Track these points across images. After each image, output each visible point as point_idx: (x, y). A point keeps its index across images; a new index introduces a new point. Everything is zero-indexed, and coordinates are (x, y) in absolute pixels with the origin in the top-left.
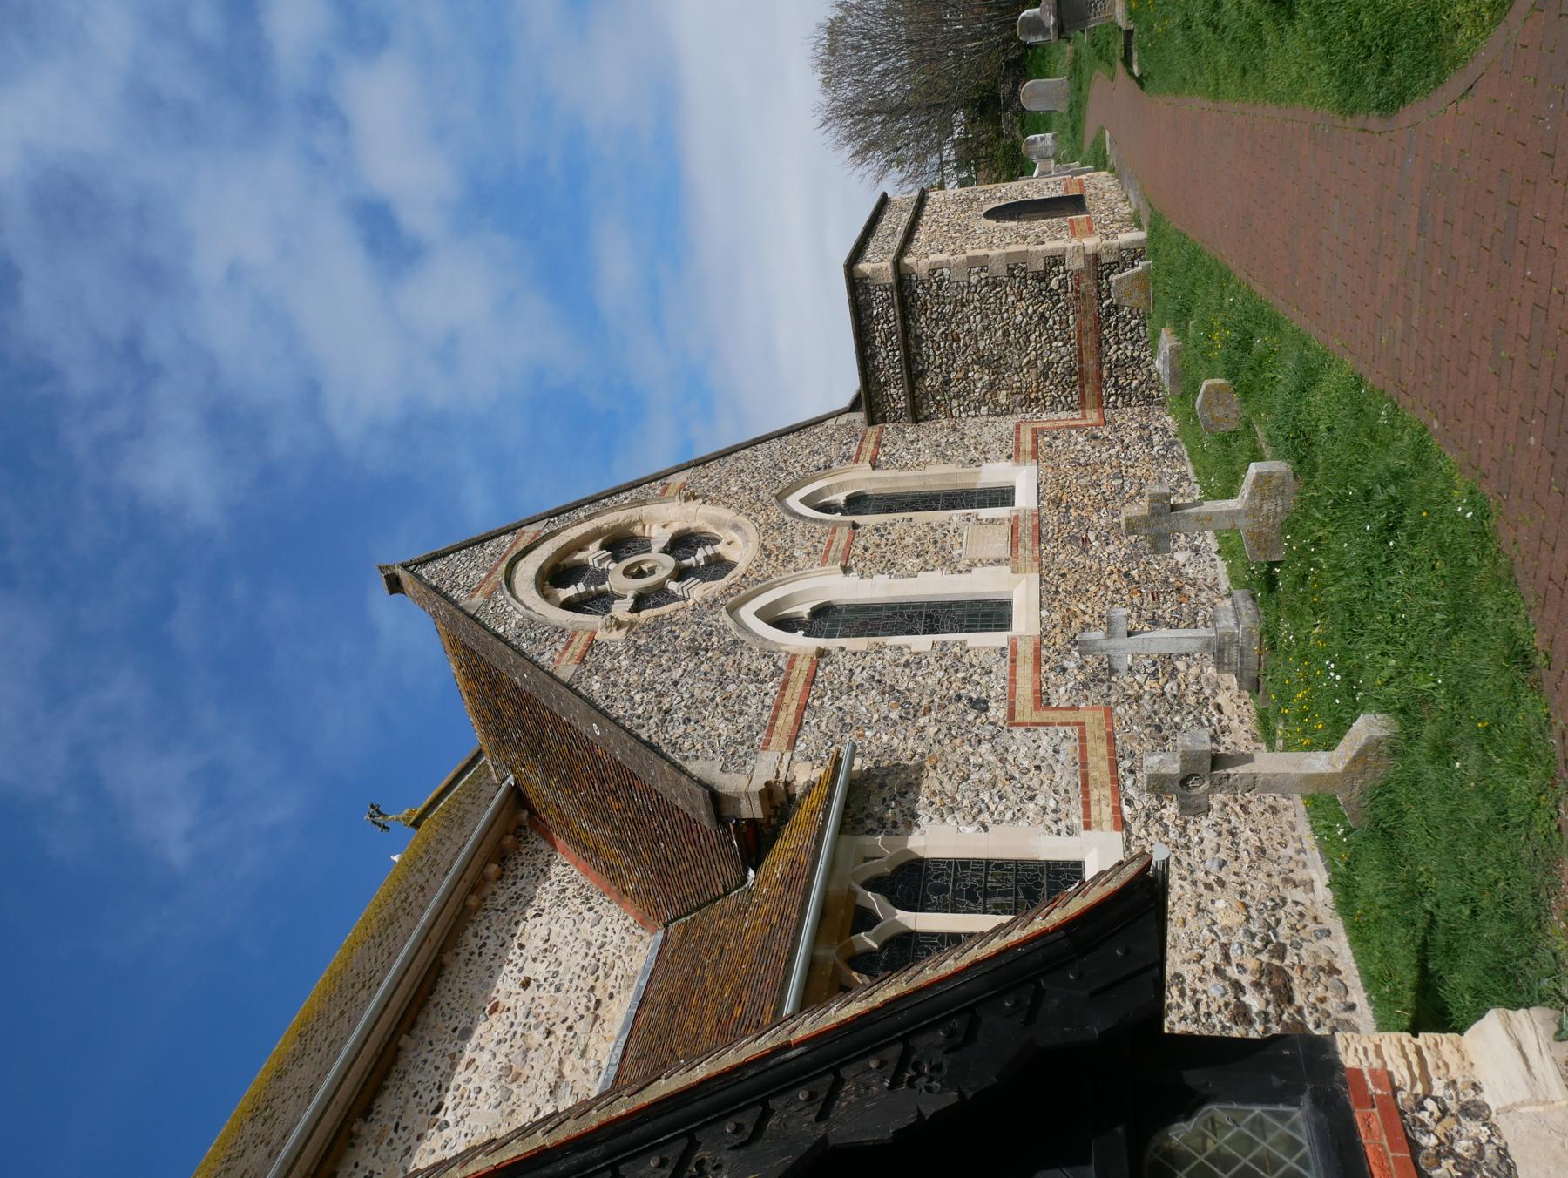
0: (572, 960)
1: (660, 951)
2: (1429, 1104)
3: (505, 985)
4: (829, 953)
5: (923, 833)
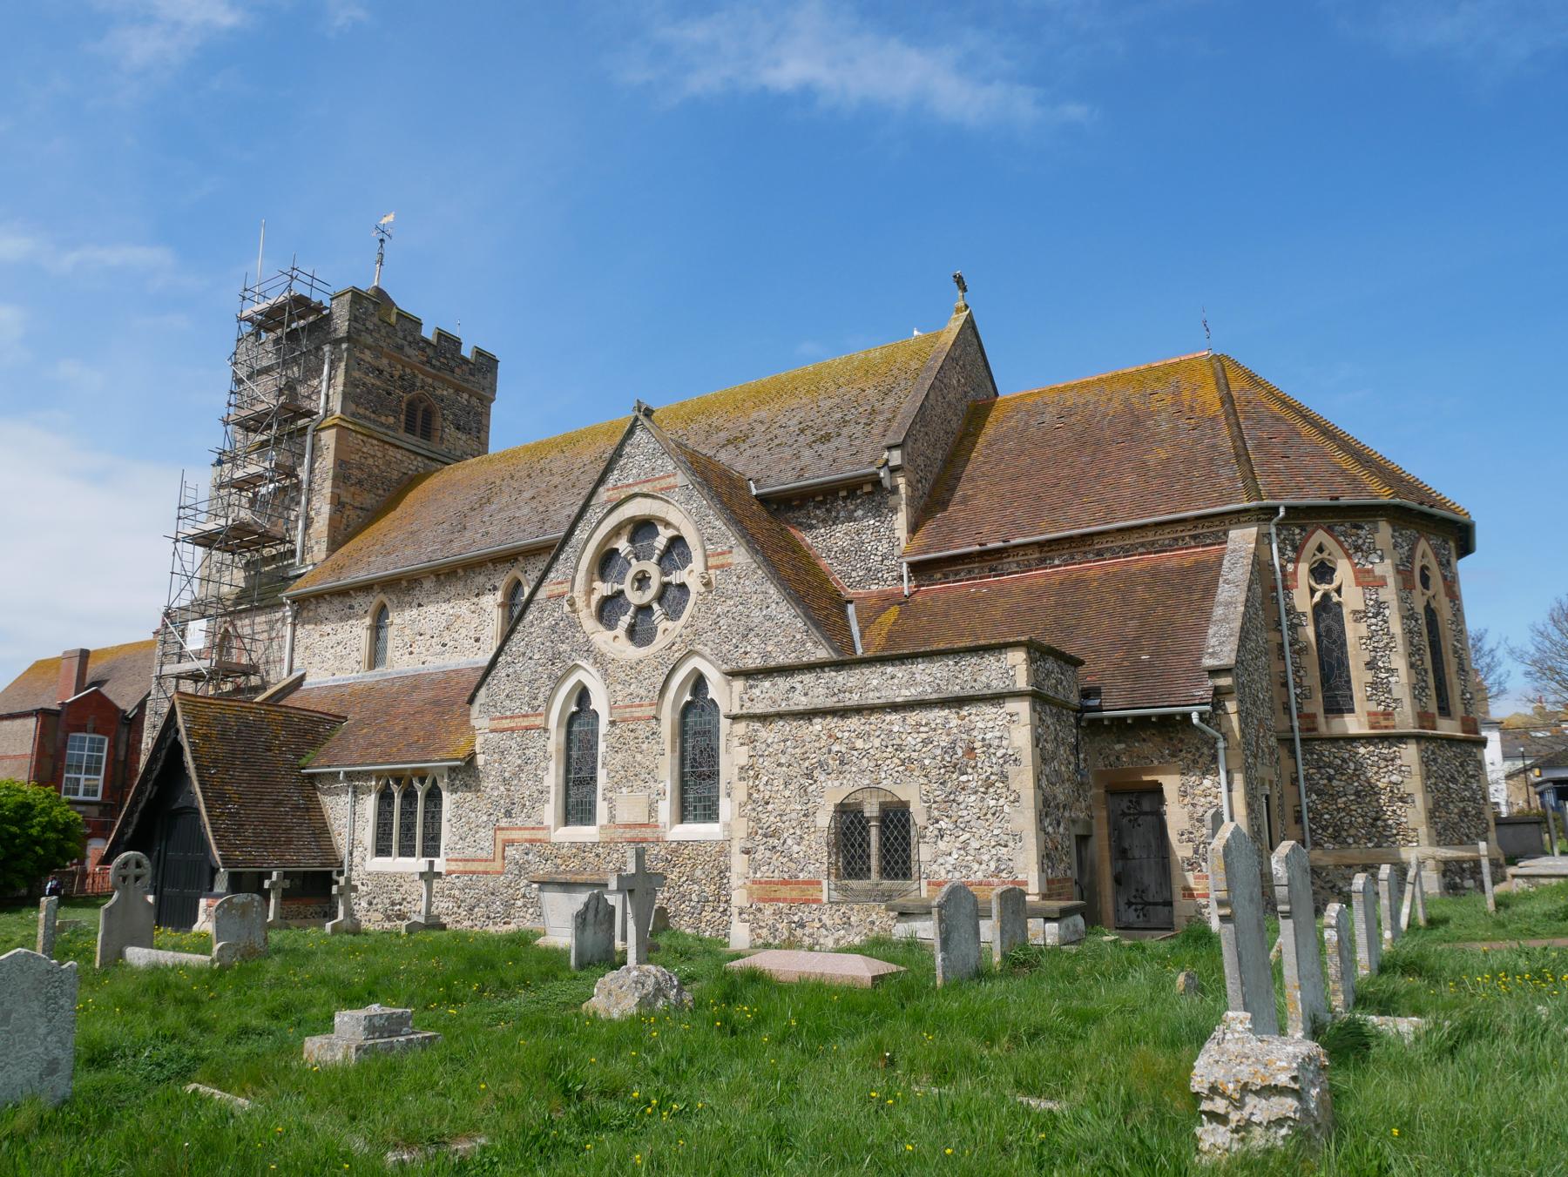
4: (409, 773)
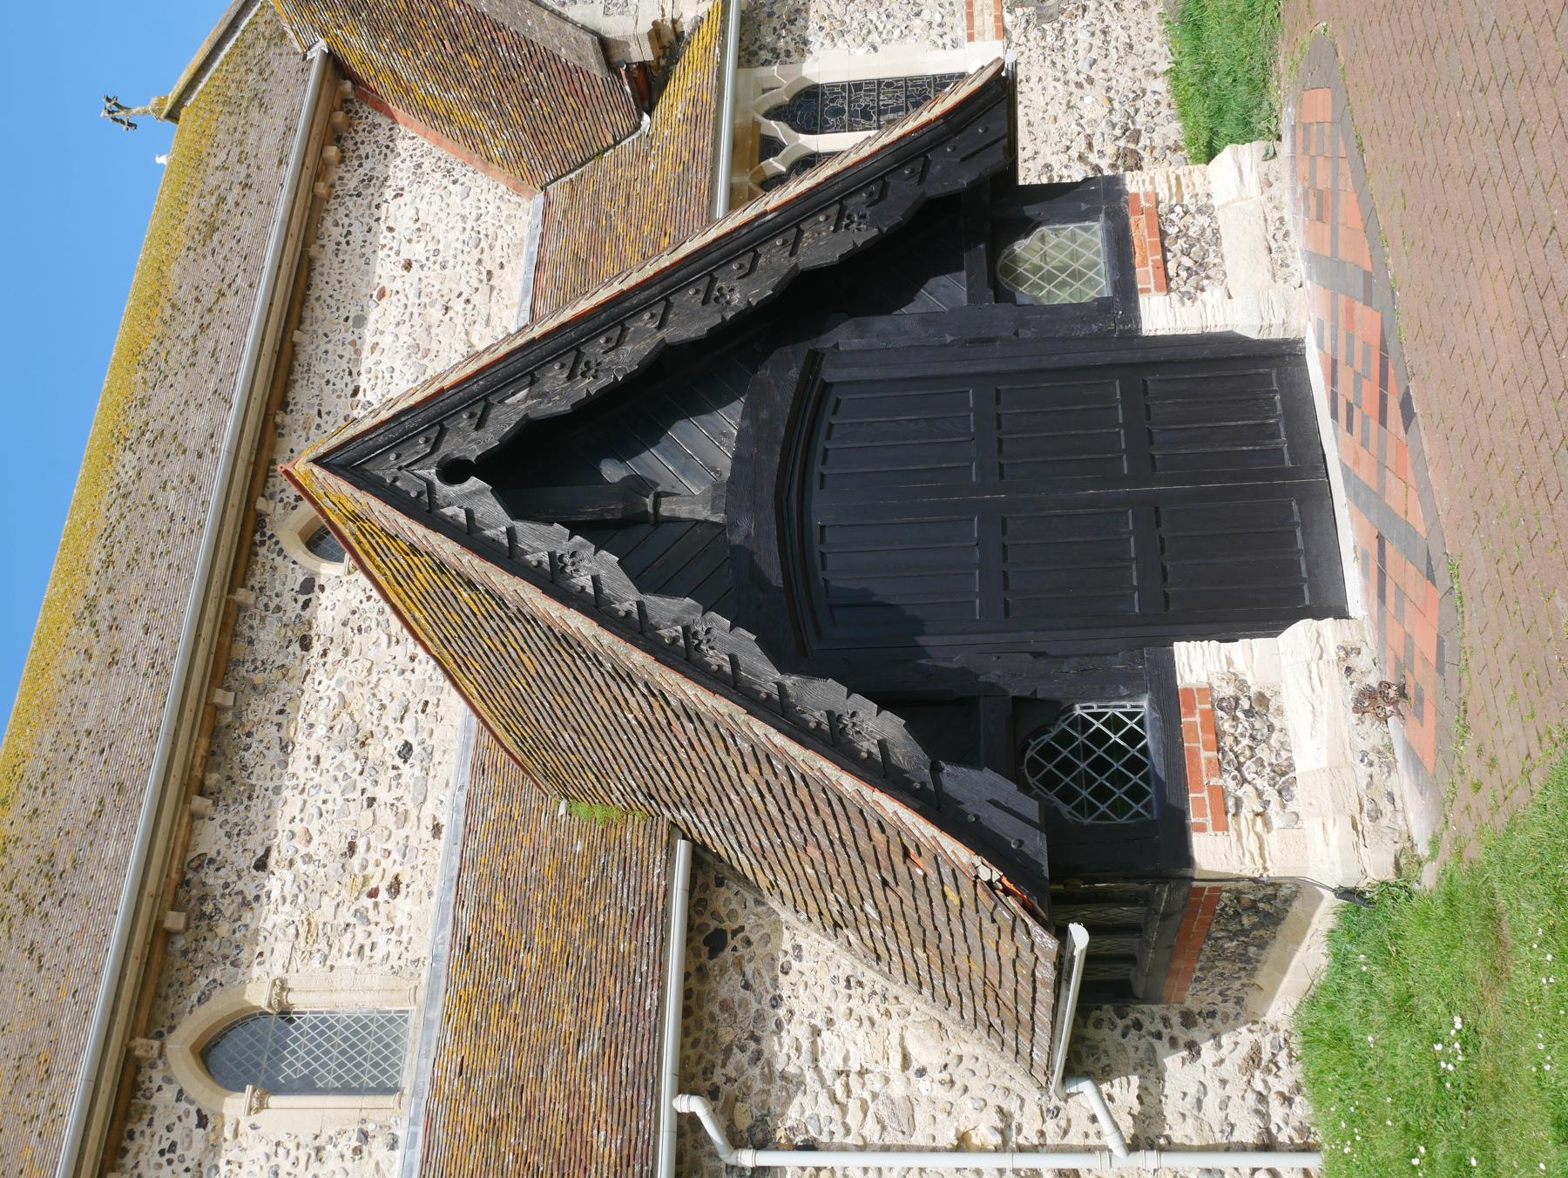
0: (451, 238)
1: (545, 215)
2: (1178, 209)
3: (385, 269)
5: (816, 60)
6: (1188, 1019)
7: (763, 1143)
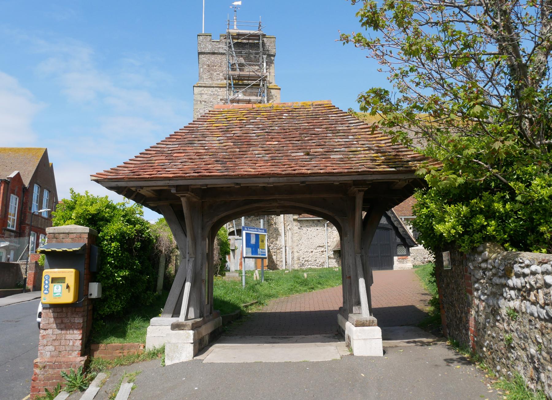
6: (338, 262)
7: (327, 226)
